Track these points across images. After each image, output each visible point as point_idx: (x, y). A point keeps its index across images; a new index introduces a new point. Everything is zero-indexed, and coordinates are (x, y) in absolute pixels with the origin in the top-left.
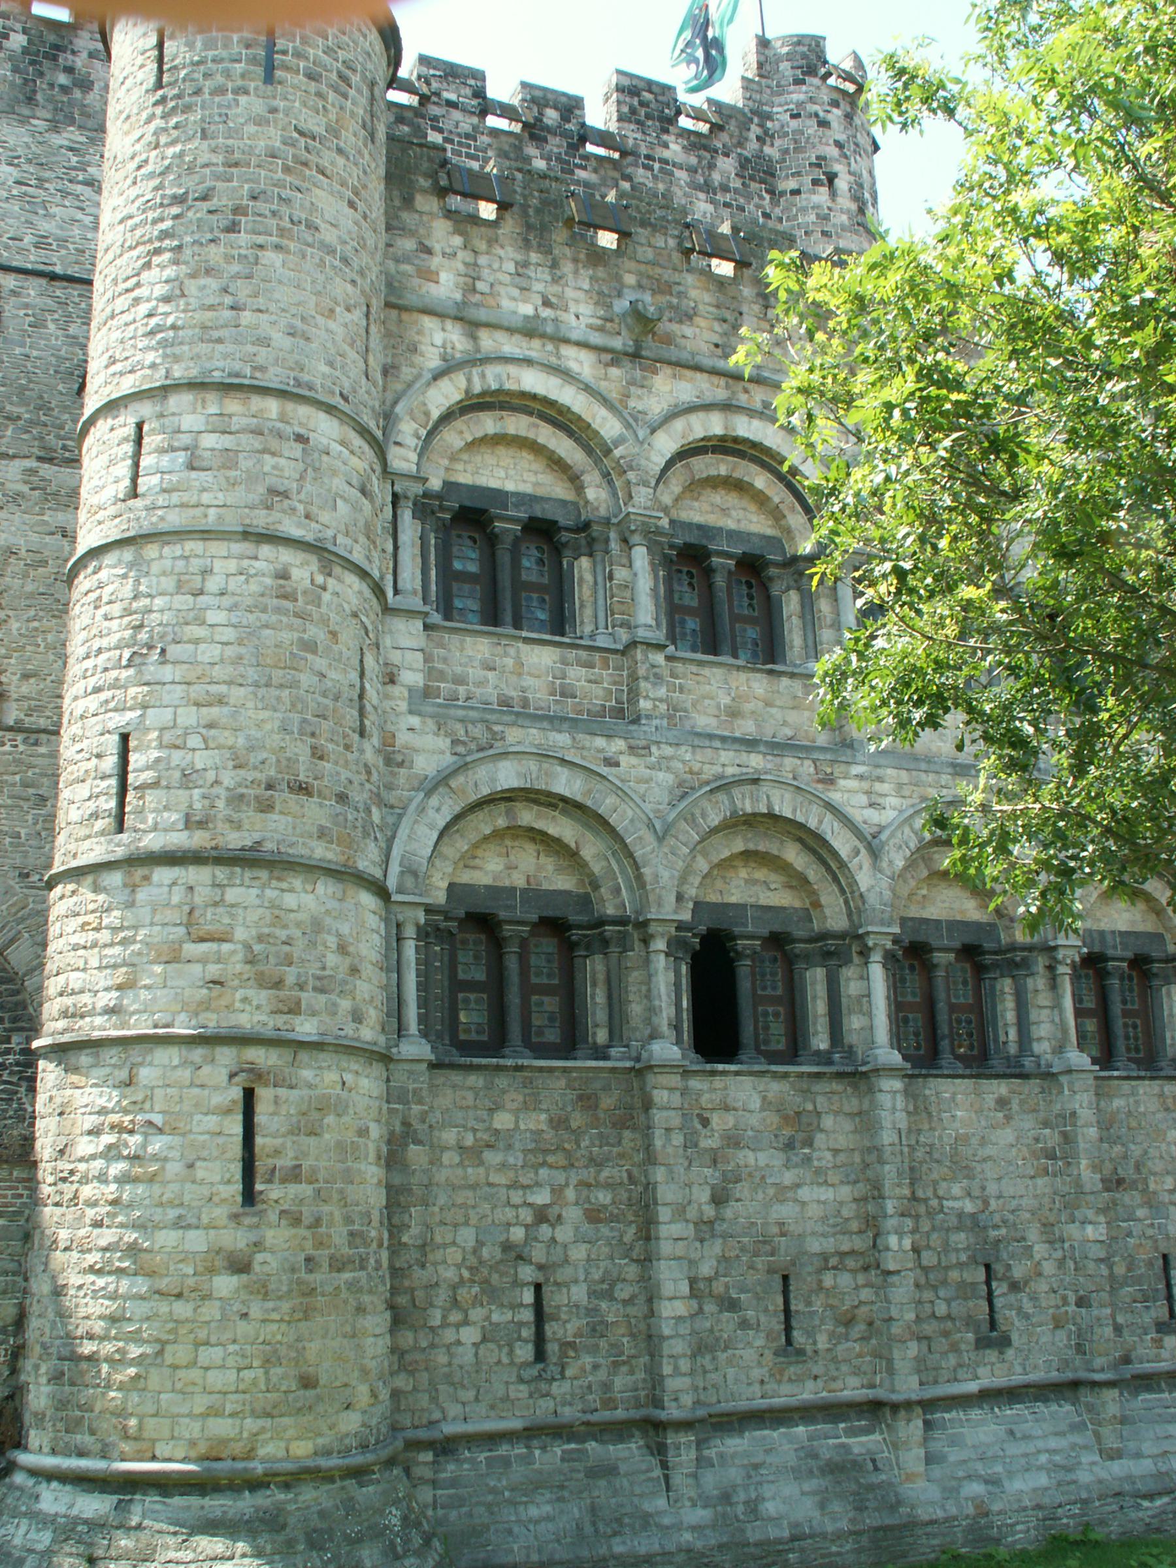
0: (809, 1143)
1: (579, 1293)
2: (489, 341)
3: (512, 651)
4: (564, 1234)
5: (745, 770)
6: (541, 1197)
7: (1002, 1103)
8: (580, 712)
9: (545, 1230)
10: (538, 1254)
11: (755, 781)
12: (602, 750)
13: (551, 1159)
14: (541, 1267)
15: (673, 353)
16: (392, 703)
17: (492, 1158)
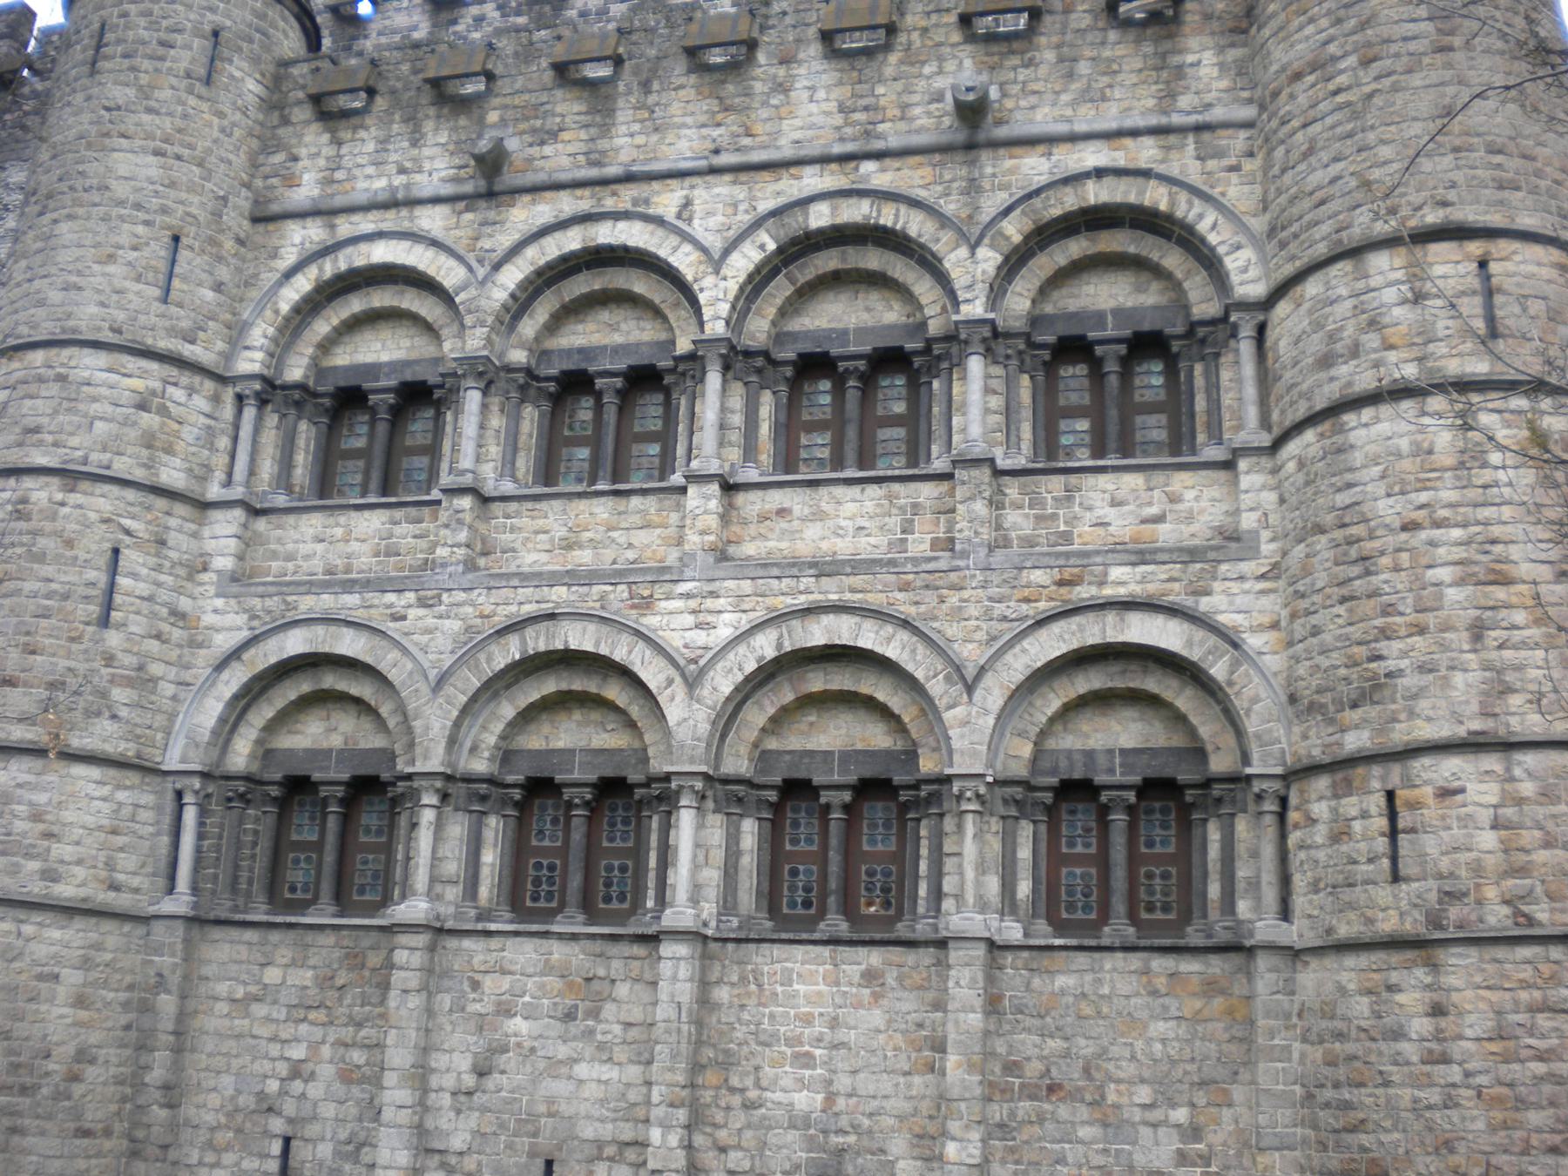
0: (594, 1014)
1: (325, 1150)
2: (346, 227)
3: (342, 520)
4: (315, 1090)
5: (544, 606)
6: (298, 1052)
7: (870, 976)
8: (402, 569)
9: (297, 1086)
10: (289, 1108)
11: (552, 616)
12: (391, 606)
13: (312, 1015)
14: (290, 1121)
15: (530, 178)
16: (201, 589)
17: (259, 1010)
